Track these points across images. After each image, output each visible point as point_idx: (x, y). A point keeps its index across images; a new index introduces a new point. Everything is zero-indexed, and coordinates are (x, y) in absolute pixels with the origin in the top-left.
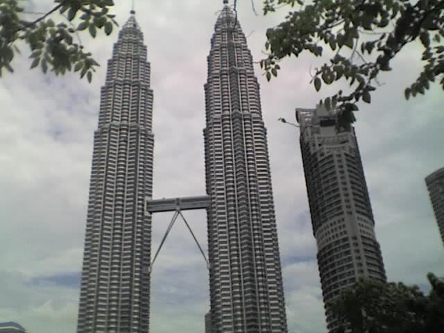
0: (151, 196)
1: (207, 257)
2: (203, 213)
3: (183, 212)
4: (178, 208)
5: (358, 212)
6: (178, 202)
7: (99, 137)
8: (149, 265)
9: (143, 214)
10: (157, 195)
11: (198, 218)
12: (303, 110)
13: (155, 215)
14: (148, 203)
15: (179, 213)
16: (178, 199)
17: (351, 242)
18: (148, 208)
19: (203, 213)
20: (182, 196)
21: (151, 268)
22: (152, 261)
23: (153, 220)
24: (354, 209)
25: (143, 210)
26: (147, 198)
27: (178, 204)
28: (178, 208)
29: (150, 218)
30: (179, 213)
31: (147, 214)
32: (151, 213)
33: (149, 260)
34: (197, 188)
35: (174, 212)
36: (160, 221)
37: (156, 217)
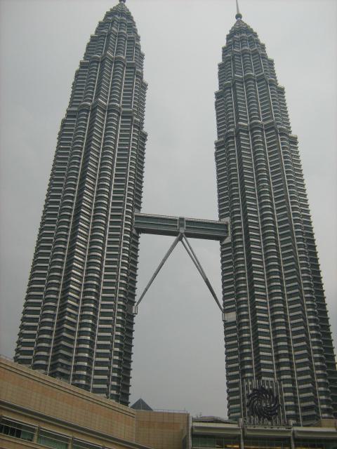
0: (139, 208)
11: (209, 252)
13: (142, 236)
16: (182, 219)
22: (137, 299)
23: (140, 240)
27: (182, 225)
28: (182, 230)
29: (138, 238)
30: (180, 239)
32: (140, 231)
33: (133, 296)
35: (173, 238)
36: (151, 246)
37: (144, 238)
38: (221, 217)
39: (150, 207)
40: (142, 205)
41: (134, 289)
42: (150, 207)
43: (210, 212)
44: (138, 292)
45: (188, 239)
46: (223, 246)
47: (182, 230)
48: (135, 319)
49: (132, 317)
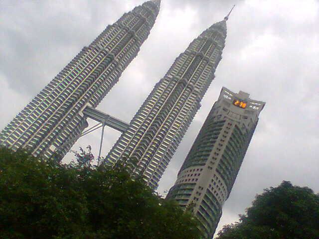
2: (119, 134)
4: (103, 120)
5: (217, 171)
6: (107, 117)
9: (77, 111)
10: (99, 108)
12: (228, 91)
14: (87, 107)
15: (103, 126)
17: (196, 188)
18: (84, 110)
19: (119, 134)
20: (112, 115)
24: (215, 167)
25: (80, 109)
34: (127, 118)
46: (121, 138)
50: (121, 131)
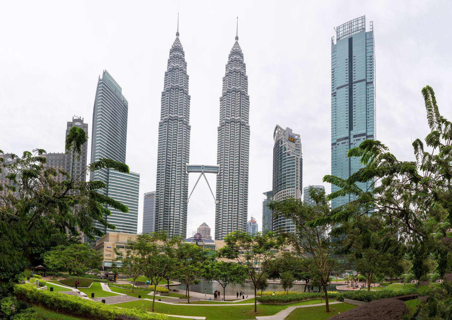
0: (188, 162)
1: (215, 198)
3: (205, 174)
7: (162, 125)
8: (187, 199)
11: (212, 178)
13: (190, 174)
21: (188, 201)
22: (188, 197)
26: (187, 164)
28: (203, 171)
29: (188, 175)
30: (203, 174)
31: (187, 173)
32: (188, 172)
33: (187, 196)
35: (200, 173)
36: (193, 177)
38: (218, 164)
39: (192, 162)
40: (189, 161)
41: (187, 194)
42: (192, 162)
43: (214, 163)
44: (189, 195)
45: (205, 173)
47: (203, 171)
48: (188, 204)
49: (187, 203)
50: (215, 173)
